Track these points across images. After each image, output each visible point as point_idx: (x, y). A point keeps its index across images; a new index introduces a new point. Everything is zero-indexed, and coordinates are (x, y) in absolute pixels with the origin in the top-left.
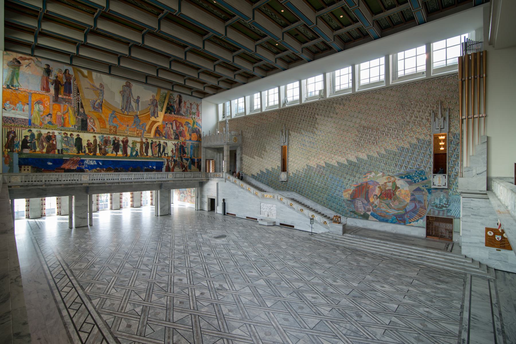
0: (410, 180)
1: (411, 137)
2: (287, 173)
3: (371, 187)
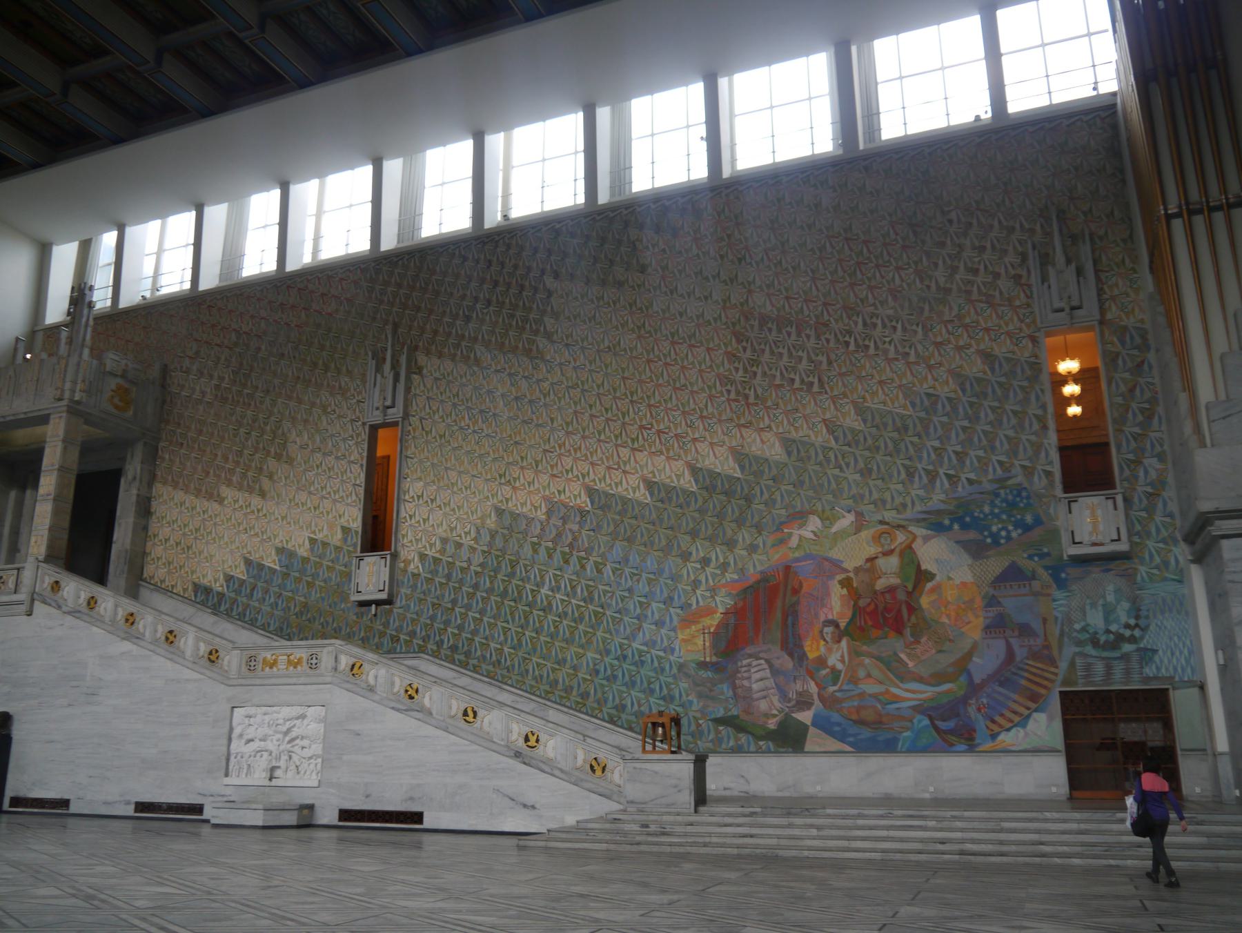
0: (972, 535)
1: (959, 349)
2: (395, 556)
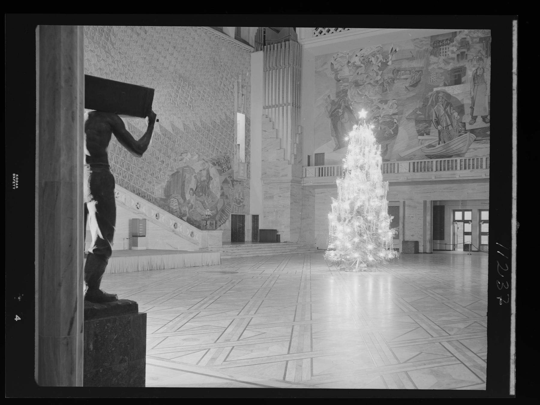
1: (221, 110)
3: (188, 176)
